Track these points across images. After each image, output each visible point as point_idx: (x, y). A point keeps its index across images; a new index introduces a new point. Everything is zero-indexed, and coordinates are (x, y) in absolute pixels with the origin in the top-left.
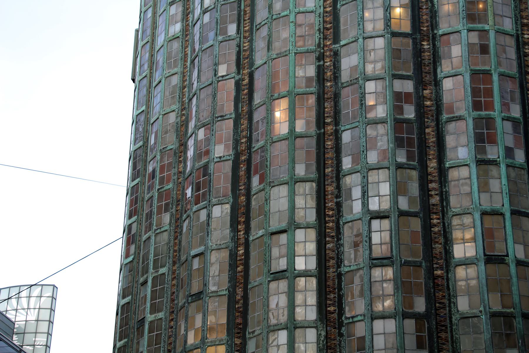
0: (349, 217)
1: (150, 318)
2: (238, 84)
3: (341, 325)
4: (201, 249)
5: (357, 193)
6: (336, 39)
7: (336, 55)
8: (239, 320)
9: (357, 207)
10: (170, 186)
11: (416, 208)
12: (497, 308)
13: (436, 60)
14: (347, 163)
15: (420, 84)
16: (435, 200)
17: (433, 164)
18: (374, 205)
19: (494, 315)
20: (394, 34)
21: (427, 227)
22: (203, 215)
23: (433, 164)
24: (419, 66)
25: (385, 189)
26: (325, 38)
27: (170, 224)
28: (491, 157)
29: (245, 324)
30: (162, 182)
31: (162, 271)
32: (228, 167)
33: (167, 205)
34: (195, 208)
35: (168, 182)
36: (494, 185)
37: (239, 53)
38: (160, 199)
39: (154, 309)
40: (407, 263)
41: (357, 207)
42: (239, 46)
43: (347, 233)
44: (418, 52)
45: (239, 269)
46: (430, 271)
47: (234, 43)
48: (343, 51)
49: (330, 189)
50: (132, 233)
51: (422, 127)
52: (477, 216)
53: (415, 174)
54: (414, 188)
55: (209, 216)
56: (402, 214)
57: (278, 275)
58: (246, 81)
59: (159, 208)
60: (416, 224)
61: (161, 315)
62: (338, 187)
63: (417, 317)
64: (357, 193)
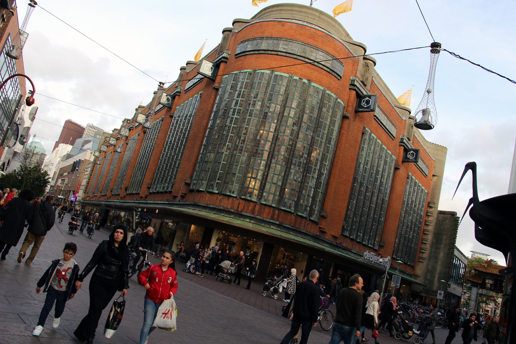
0: (290, 178)
1: (237, 174)
2: (274, 135)
3: (283, 198)
4: (258, 168)
5: (293, 174)
6: (297, 138)
7: (296, 142)
8: (262, 187)
9: (292, 177)
10: (249, 147)
11: (300, 181)
12: (306, 204)
13: (311, 153)
14: (292, 167)
15: (308, 156)
16: (303, 180)
17: (305, 173)
18: (295, 178)
19: (305, 205)
20: (308, 144)
21: (301, 185)
22: (259, 161)
23: (305, 173)
24: (309, 152)
25: (298, 176)
26: (295, 137)
27: (247, 156)
28: (314, 176)
29: (264, 189)
30: (247, 144)
31: (243, 166)
32: (268, 153)
33: (247, 151)
34: (257, 158)
35: (248, 145)
36: (312, 181)
37: (276, 128)
38: (245, 148)
39: (239, 173)
40: (297, 191)
41: (292, 177)
42: (276, 126)
43: (289, 181)
44: (309, 149)
45: (265, 177)
46: (299, 193)
47: (275, 125)
48: (298, 142)
49: (288, 170)
50: (229, 147)
51: (306, 166)
52: (309, 187)
53: (302, 174)
54: (301, 178)
55: (261, 162)
56: (299, 182)
57: (274, 183)
58: (276, 136)
59: (245, 151)
60: (300, 184)
61: (241, 175)
62: (289, 171)
63: (294, 201)
64: (293, 174)
